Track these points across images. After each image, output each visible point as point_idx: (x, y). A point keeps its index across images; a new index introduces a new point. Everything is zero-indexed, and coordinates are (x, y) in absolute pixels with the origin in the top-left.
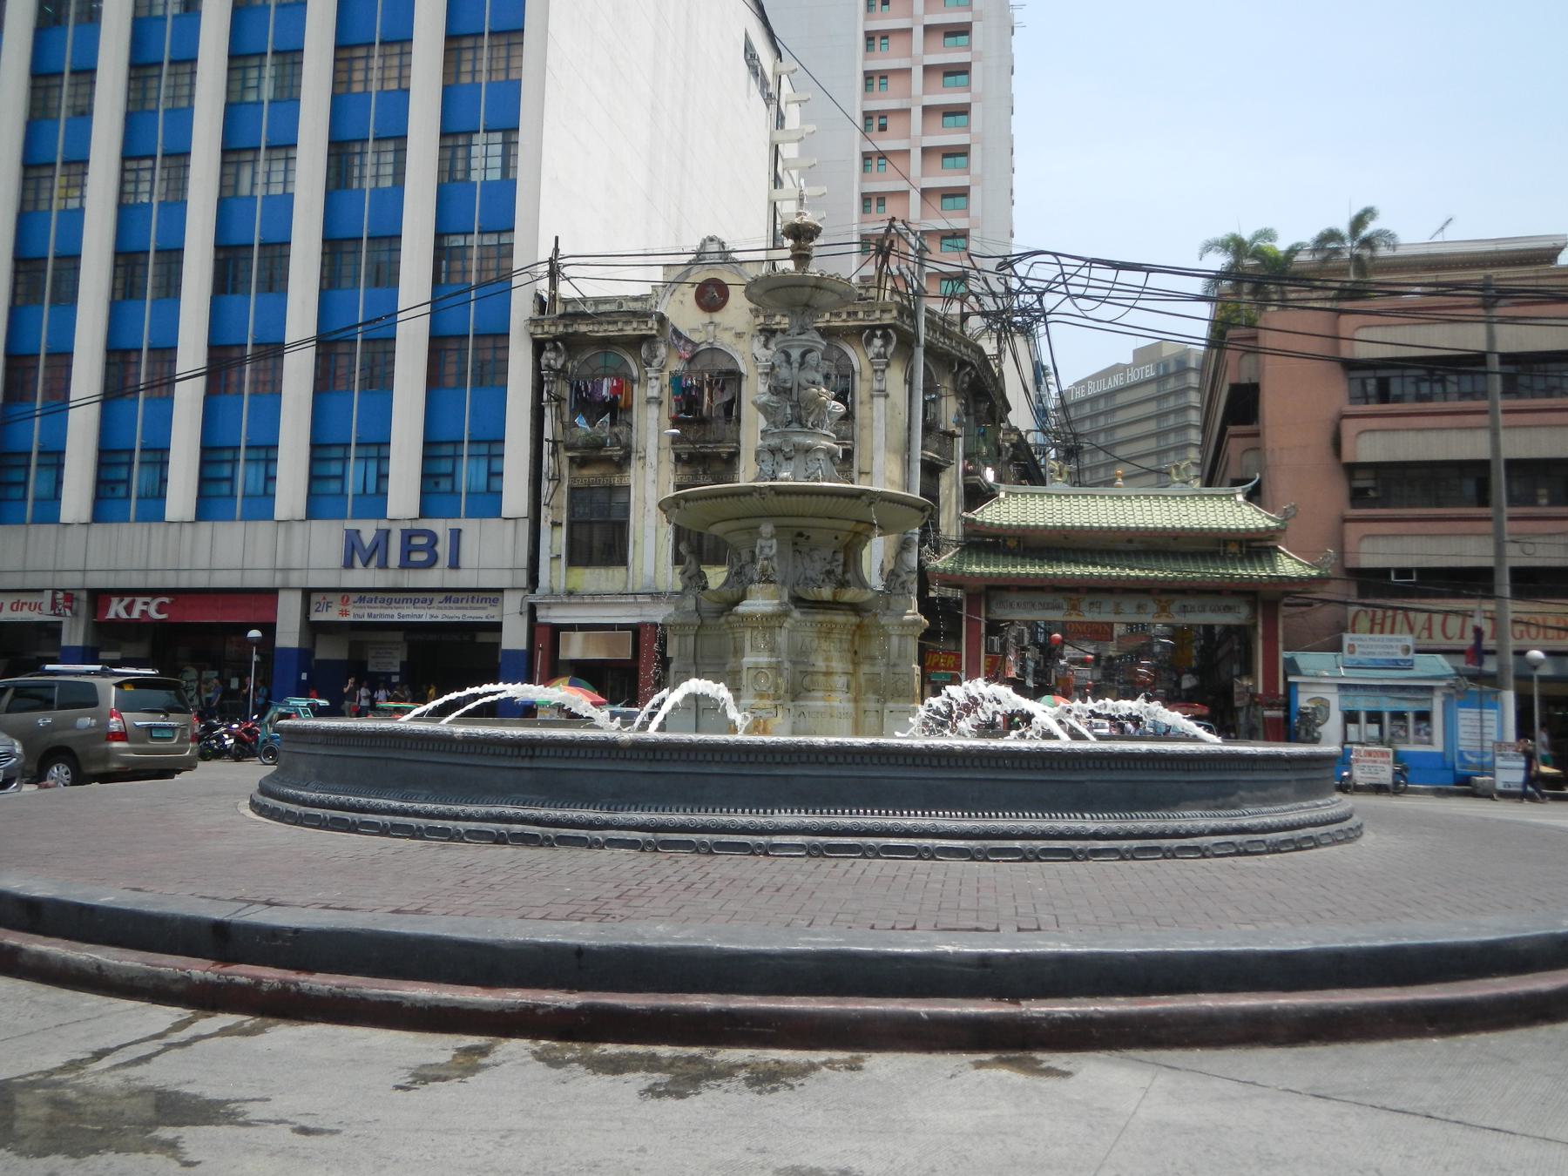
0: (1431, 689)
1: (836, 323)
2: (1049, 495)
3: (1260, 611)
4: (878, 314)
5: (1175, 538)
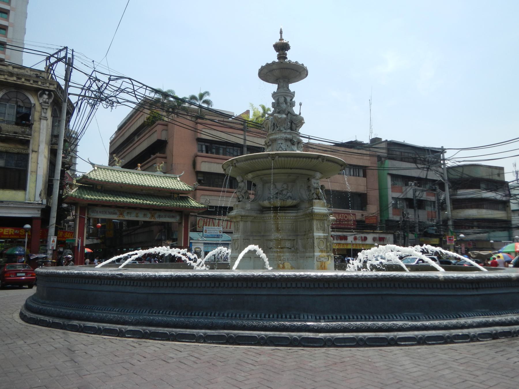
0: (228, 244)
1: (27, 84)
2: (114, 170)
3: (183, 218)
4: (48, 85)
5: (159, 191)
